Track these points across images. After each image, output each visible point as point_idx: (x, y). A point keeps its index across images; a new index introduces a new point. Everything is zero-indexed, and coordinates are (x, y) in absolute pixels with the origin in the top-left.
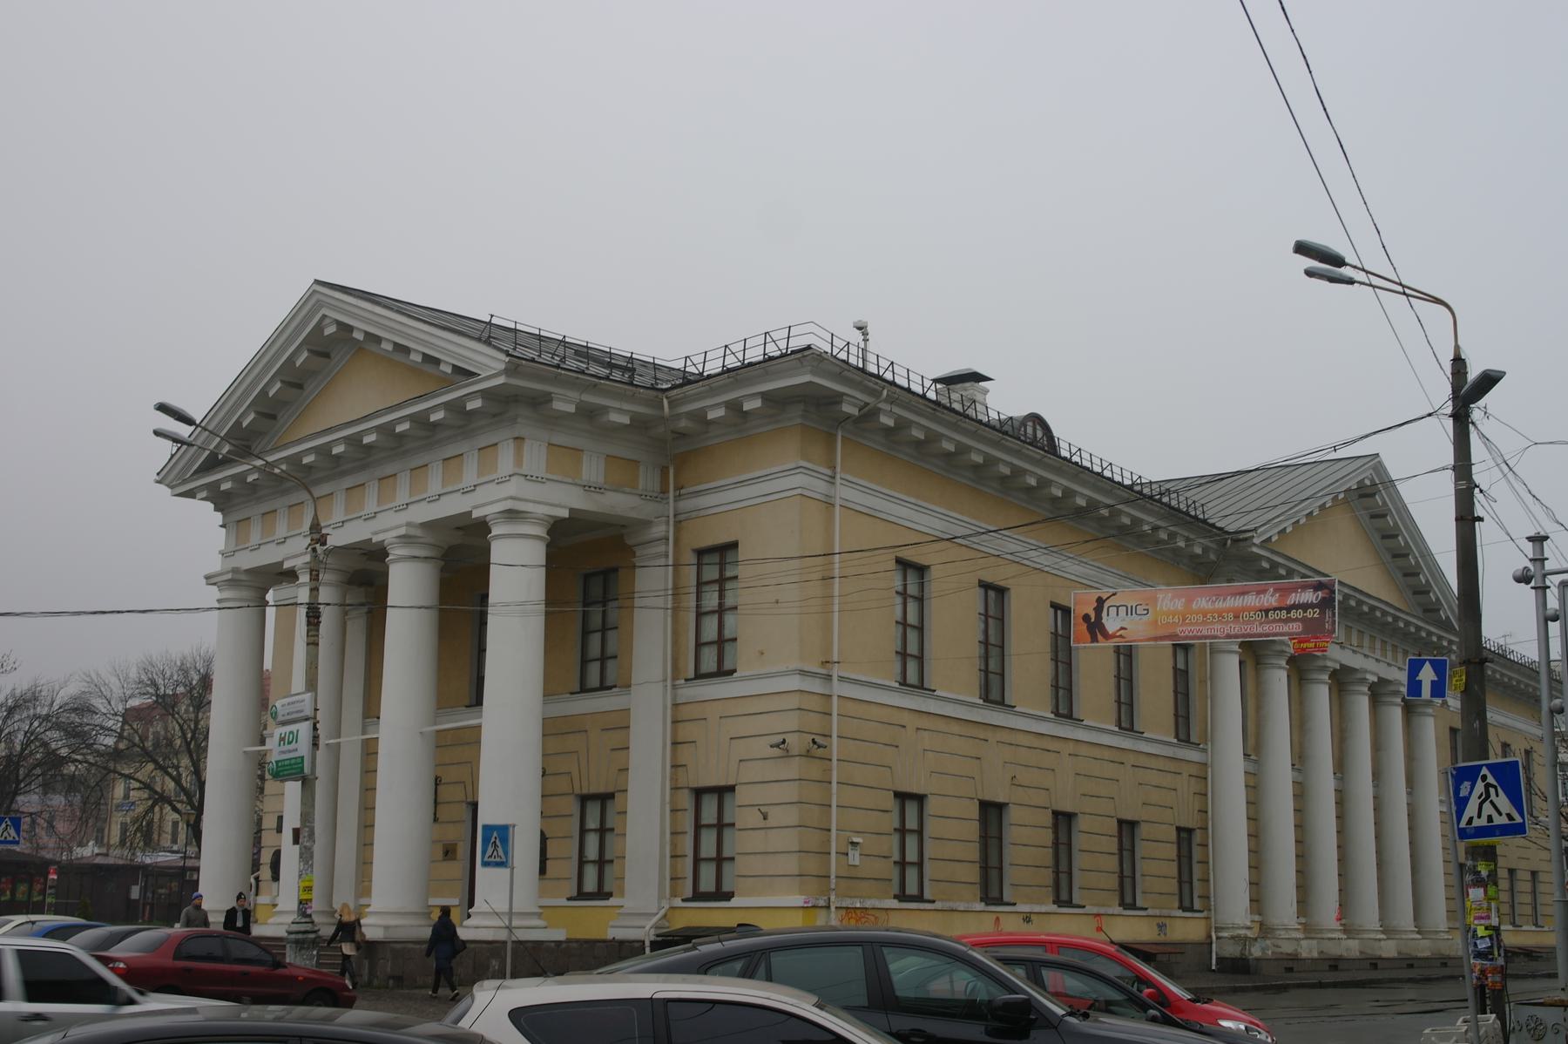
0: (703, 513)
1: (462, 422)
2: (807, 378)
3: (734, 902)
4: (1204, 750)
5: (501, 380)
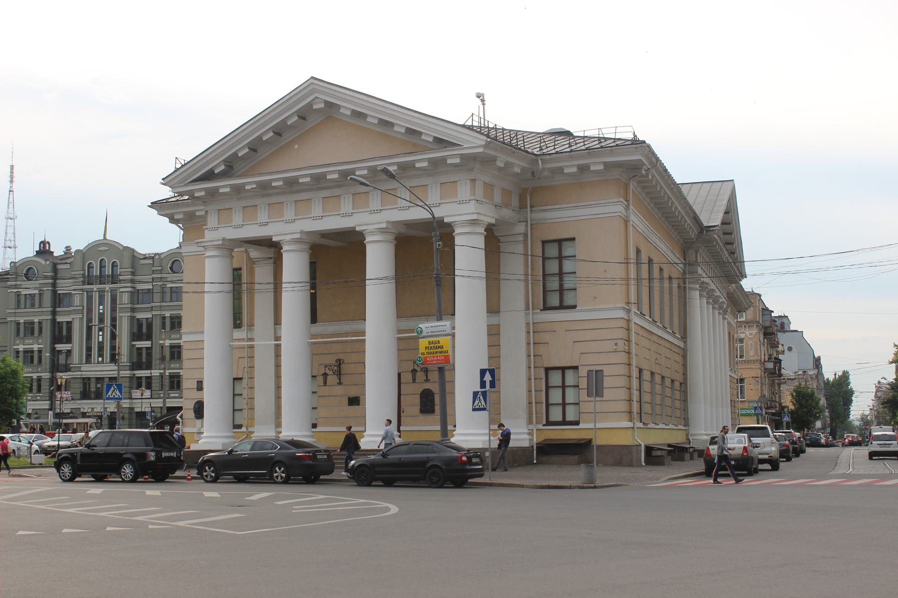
0: (549, 221)
2: (639, 157)
3: (581, 426)
4: (685, 342)
5: (481, 150)
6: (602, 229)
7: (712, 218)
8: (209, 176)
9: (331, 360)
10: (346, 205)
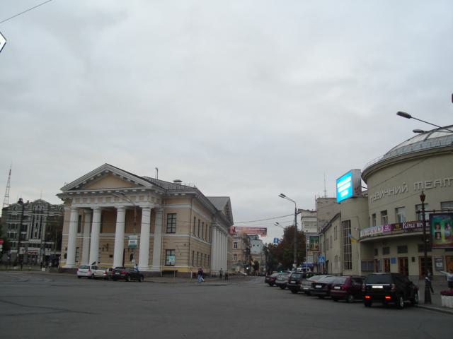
1: (139, 191)
6: (184, 210)
7: (221, 208)
8: (74, 189)
9: (105, 244)
10: (113, 200)
